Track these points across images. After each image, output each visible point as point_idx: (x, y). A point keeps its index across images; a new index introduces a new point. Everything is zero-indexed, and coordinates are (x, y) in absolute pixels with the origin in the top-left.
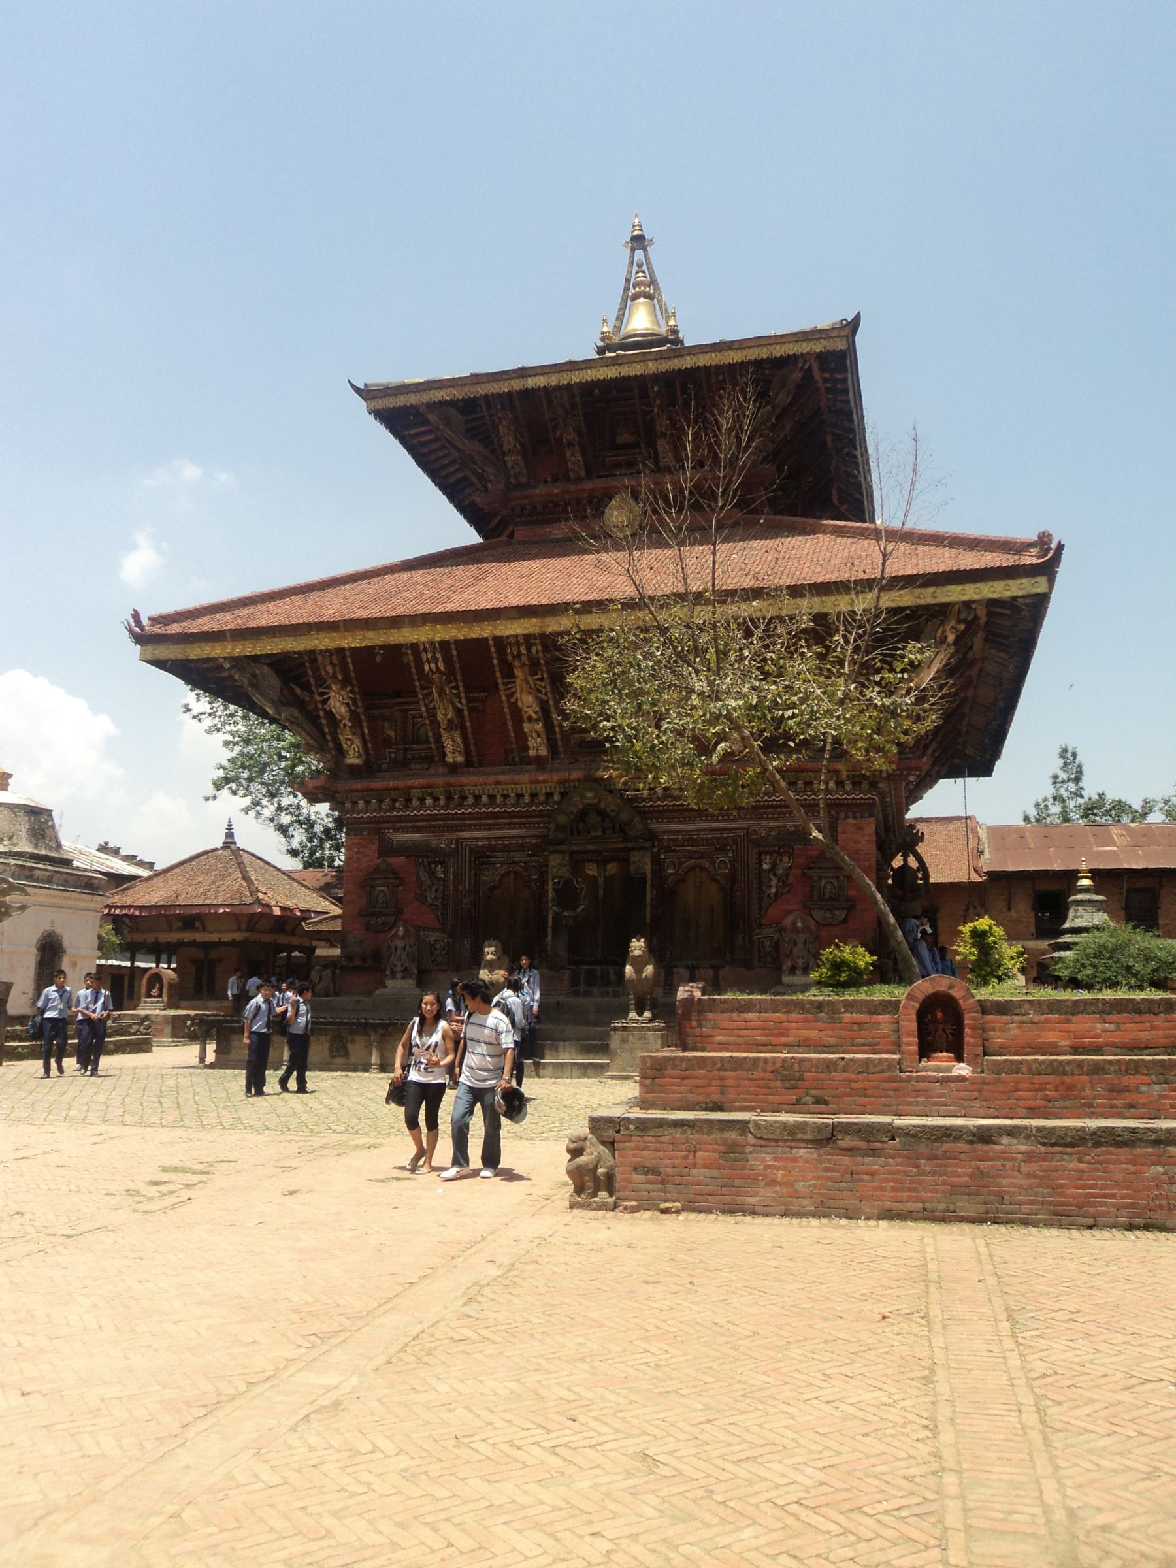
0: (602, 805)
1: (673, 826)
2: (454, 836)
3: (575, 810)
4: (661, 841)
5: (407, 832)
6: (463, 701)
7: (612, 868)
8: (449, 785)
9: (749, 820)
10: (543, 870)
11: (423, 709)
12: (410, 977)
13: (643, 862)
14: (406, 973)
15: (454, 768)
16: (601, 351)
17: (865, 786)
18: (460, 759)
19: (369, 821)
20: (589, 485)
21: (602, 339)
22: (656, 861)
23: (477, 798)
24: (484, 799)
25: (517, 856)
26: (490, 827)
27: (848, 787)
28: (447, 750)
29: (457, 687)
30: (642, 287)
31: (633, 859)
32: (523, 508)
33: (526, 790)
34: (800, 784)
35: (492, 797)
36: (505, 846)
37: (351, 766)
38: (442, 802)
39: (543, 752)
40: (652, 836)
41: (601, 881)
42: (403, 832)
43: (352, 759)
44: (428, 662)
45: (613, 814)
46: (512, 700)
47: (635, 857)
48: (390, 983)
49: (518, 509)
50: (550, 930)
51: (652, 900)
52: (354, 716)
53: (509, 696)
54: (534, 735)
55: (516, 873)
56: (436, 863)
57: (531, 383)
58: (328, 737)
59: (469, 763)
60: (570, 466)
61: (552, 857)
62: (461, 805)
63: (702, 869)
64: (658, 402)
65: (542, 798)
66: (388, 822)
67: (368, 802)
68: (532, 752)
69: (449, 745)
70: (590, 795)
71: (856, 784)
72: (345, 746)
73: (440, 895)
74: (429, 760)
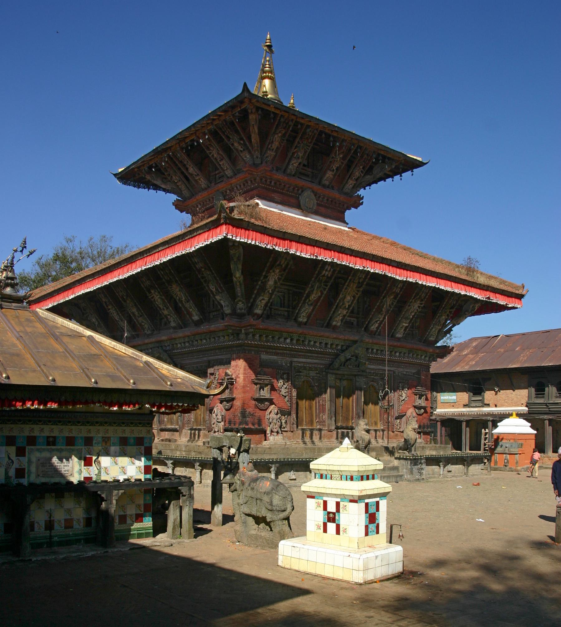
2: (289, 359)
7: (345, 383)
15: (300, 324)
18: (305, 320)
24: (312, 343)
25: (312, 373)
27: (427, 358)
29: (326, 286)
35: (315, 342)
36: (310, 367)
37: (256, 314)
38: (295, 342)
41: (342, 389)
42: (270, 355)
48: (271, 438)
56: (284, 374)
59: (305, 324)
60: (290, 167)
65: (334, 346)
67: (260, 336)
68: (334, 323)
71: (430, 358)
74: (288, 318)
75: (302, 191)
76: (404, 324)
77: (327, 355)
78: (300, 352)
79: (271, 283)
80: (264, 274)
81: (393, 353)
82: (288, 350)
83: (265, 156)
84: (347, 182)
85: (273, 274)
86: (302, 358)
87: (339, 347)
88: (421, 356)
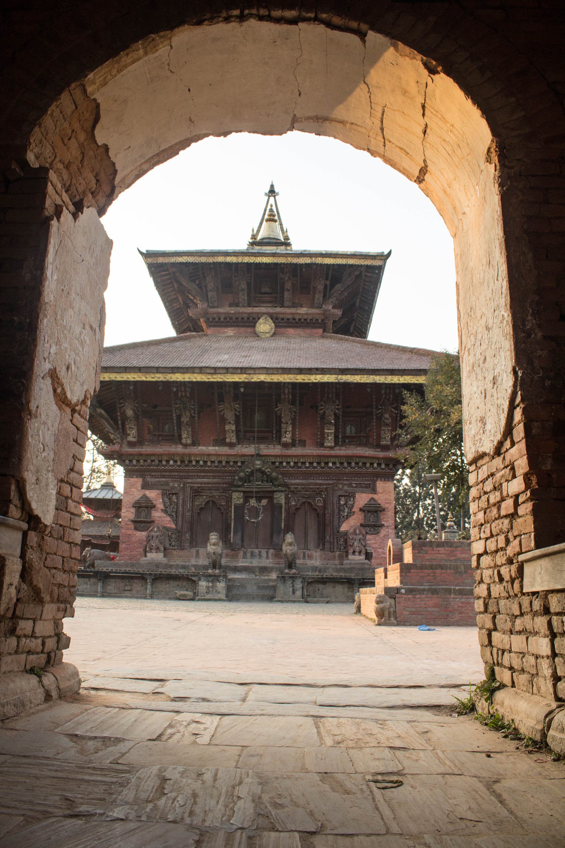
0: (264, 469)
1: (297, 481)
3: (250, 470)
4: (289, 488)
5: (157, 478)
6: (196, 412)
7: (264, 502)
8: (184, 454)
9: (334, 480)
10: (229, 500)
11: (174, 415)
12: (160, 552)
13: (280, 498)
14: (158, 549)
16: (252, 244)
17: (391, 466)
18: (189, 441)
19: (137, 471)
20: (249, 310)
21: (252, 238)
22: (287, 498)
23: (198, 462)
24: (201, 463)
25: (215, 493)
26: (203, 477)
27: (383, 466)
28: (183, 436)
30: (272, 217)
31: (275, 496)
32: (214, 319)
33: (224, 459)
34: (361, 464)
35: (205, 462)
38: (179, 463)
39: (234, 440)
40: (286, 485)
42: (156, 478)
43: (130, 438)
44: (181, 391)
45: (268, 473)
46: (222, 413)
47: (276, 495)
49: (211, 320)
50: (232, 530)
51: (285, 517)
52: (137, 417)
53: (220, 412)
54: (231, 432)
55: (213, 502)
56: (173, 494)
57: (229, 259)
58: (120, 426)
61: (234, 494)
62: (187, 466)
63: (309, 503)
64: (288, 275)
65: (231, 463)
66: (148, 471)
67: (138, 461)
69: (184, 436)
70: (258, 462)
71: (387, 465)
72: (128, 432)
73: (175, 510)
75: (259, 319)
76: (327, 431)
77: (229, 472)
78: (193, 472)
79: (130, 413)
80: (118, 405)
81: (323, 465)
82: (176, 472)
83: (209, 298)
84: (314, 298)
85: (127, 404)
86: (196, 478)
87: (239, 464)
88: (372, 464)
